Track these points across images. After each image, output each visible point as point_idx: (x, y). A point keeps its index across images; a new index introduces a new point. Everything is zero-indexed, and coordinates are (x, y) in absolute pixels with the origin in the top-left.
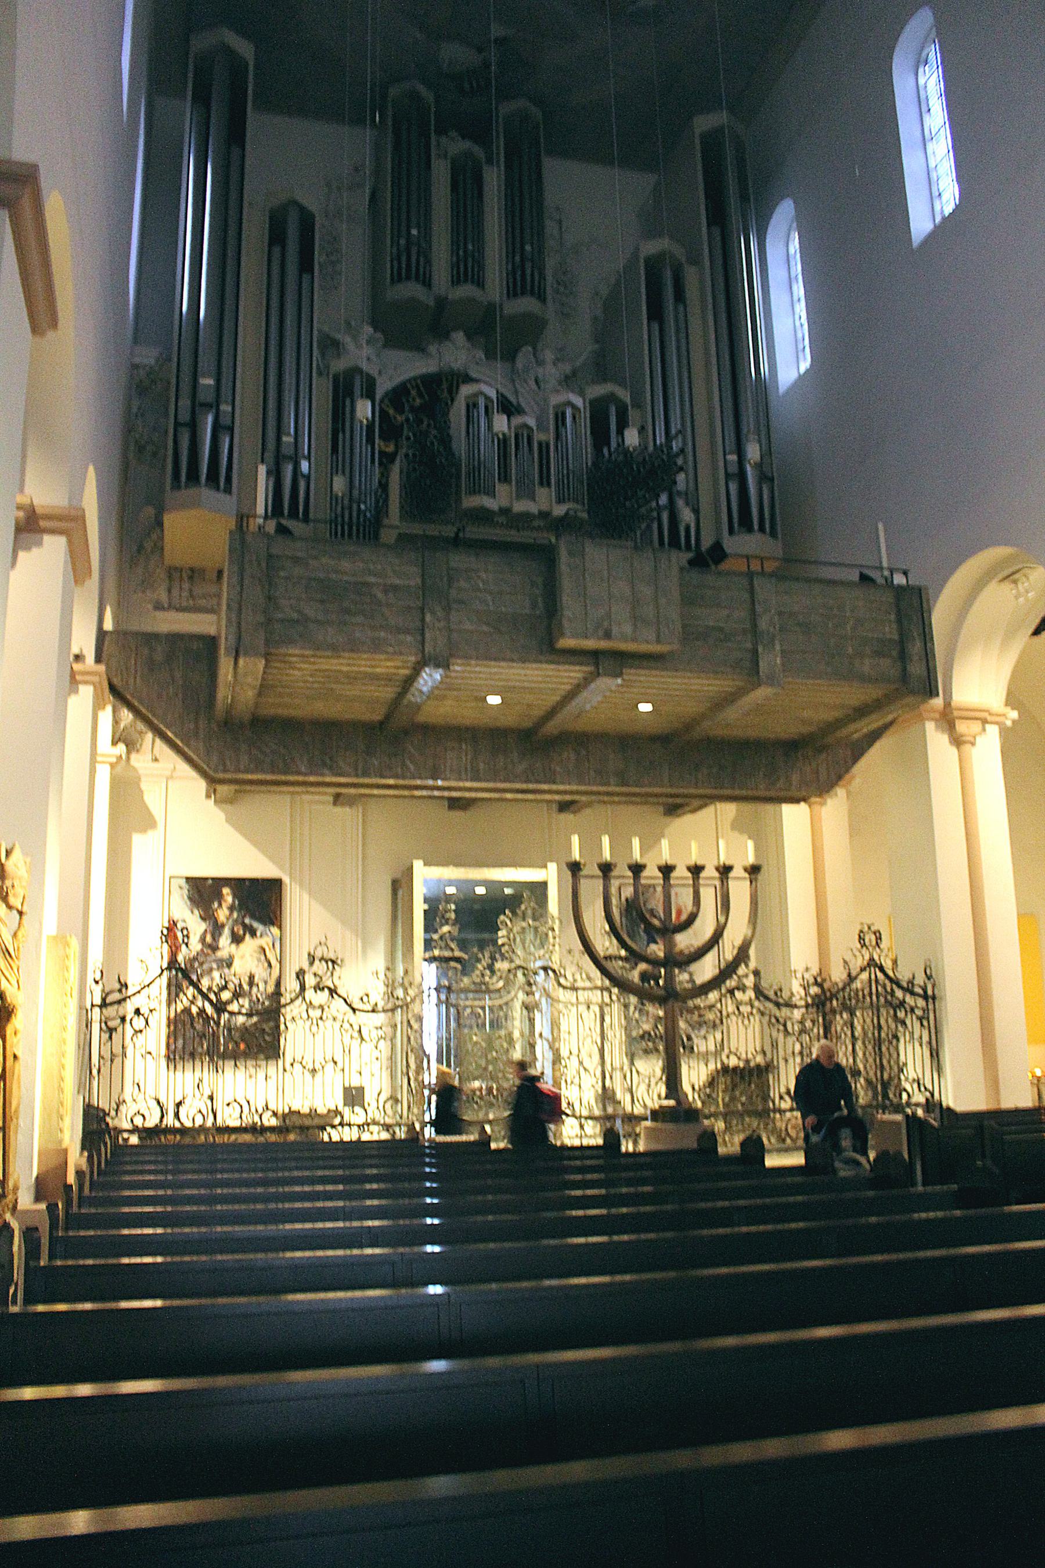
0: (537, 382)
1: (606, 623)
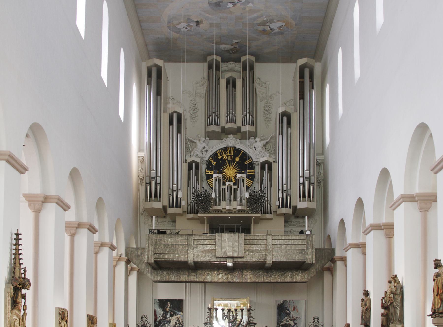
0: (255, 148)
1: (226, 253)
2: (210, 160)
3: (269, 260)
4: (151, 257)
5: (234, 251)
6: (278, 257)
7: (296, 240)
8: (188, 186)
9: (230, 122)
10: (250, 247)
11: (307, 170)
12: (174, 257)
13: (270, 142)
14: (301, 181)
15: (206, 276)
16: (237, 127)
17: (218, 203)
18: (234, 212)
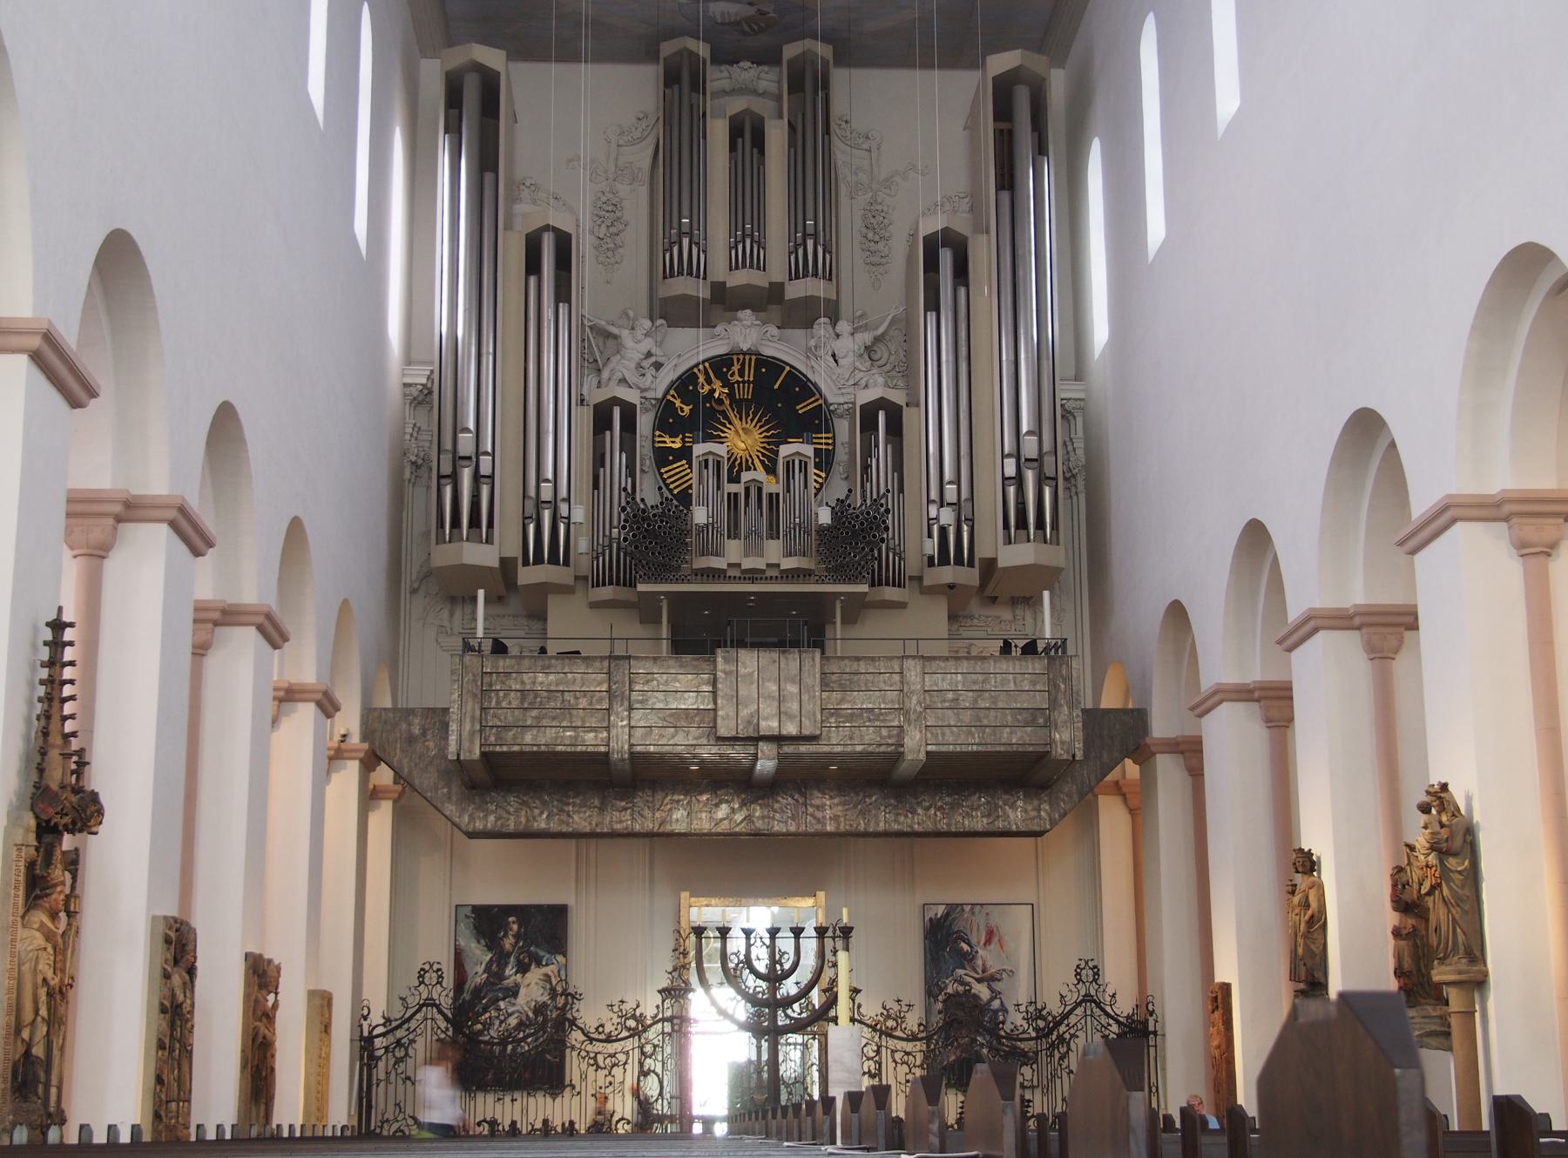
0: (834, 356)
1: (755, 721)
2: (669, 397)
3: (916, 745)
4: (472, 742)
5: (786, 714)
6: (946, 738)
7: (1011, 677)
8: (596, 486)
9: (744, 266)
10: (842, 701)
11: (1029, 433)
12: (557, 738)
13: (887, 338)
14: (1010, 470)
15: (670, 809)
16: (770, 283)
17: (713, 547)
18: (771, 577)
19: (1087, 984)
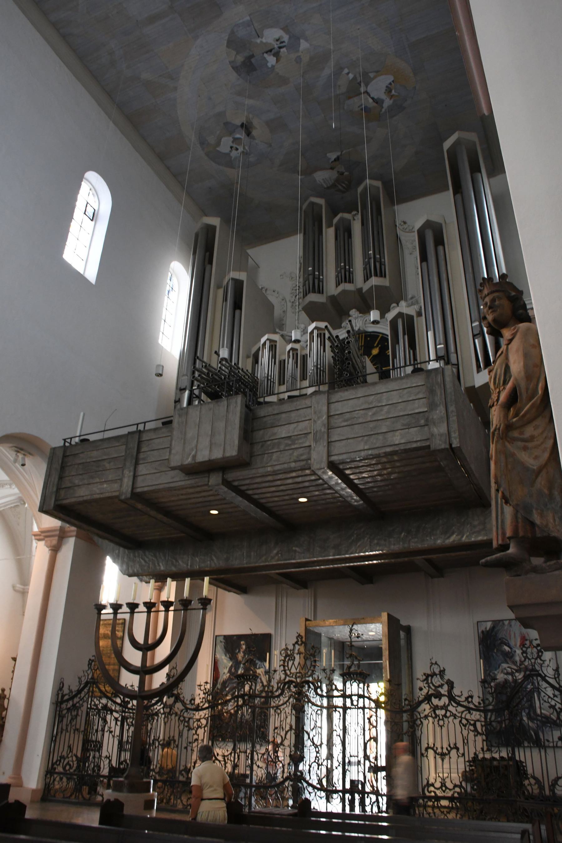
19: (533, 661)
